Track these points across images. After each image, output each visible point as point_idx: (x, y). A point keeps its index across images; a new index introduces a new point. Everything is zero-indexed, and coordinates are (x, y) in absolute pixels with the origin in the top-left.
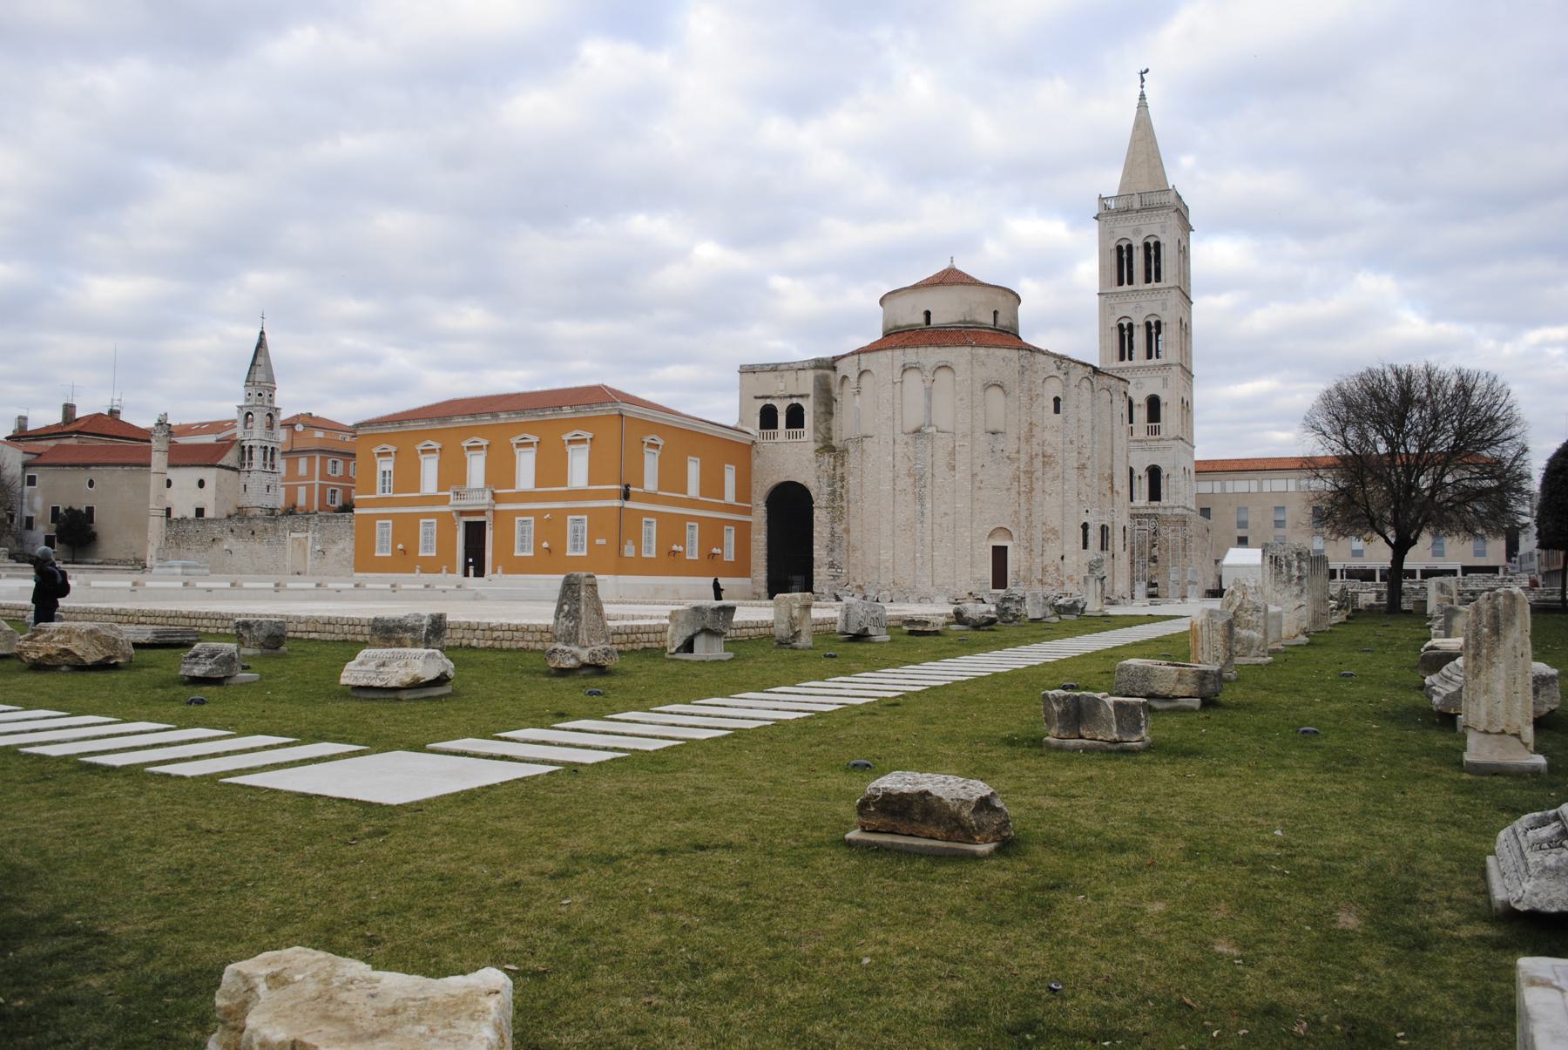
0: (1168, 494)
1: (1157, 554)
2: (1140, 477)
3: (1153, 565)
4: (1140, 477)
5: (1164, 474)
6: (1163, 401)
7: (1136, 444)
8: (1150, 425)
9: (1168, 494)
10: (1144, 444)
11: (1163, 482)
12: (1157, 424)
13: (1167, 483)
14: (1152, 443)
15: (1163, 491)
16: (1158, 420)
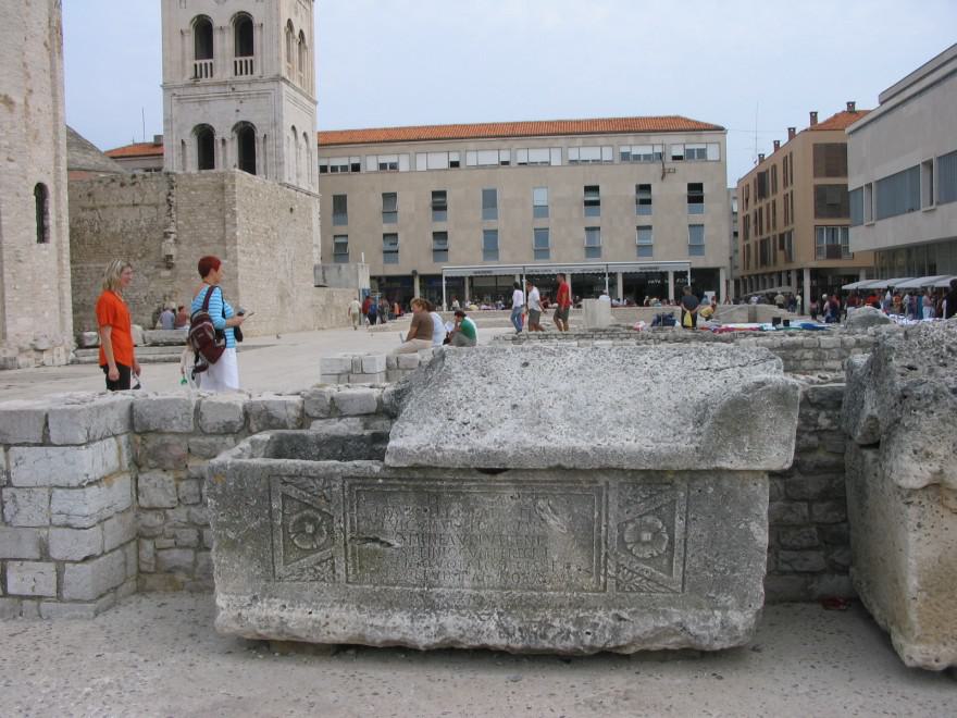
0: (265, 166)
1: (173, 251)
2: (224, 141)
3: (166, 273)
4: (224, 141)
5: (259, 135)
6: (256, 21)
7: (217, 89)
8: (238, 59)
9: (265, 166)
10: (228, 89)
11: (259, 147)
12: (249, 58)
13: (265, 148)
14: (239, 88)
15: (259, 161)
16: (250, 52)
